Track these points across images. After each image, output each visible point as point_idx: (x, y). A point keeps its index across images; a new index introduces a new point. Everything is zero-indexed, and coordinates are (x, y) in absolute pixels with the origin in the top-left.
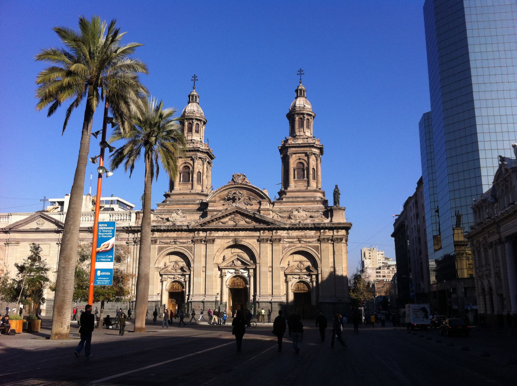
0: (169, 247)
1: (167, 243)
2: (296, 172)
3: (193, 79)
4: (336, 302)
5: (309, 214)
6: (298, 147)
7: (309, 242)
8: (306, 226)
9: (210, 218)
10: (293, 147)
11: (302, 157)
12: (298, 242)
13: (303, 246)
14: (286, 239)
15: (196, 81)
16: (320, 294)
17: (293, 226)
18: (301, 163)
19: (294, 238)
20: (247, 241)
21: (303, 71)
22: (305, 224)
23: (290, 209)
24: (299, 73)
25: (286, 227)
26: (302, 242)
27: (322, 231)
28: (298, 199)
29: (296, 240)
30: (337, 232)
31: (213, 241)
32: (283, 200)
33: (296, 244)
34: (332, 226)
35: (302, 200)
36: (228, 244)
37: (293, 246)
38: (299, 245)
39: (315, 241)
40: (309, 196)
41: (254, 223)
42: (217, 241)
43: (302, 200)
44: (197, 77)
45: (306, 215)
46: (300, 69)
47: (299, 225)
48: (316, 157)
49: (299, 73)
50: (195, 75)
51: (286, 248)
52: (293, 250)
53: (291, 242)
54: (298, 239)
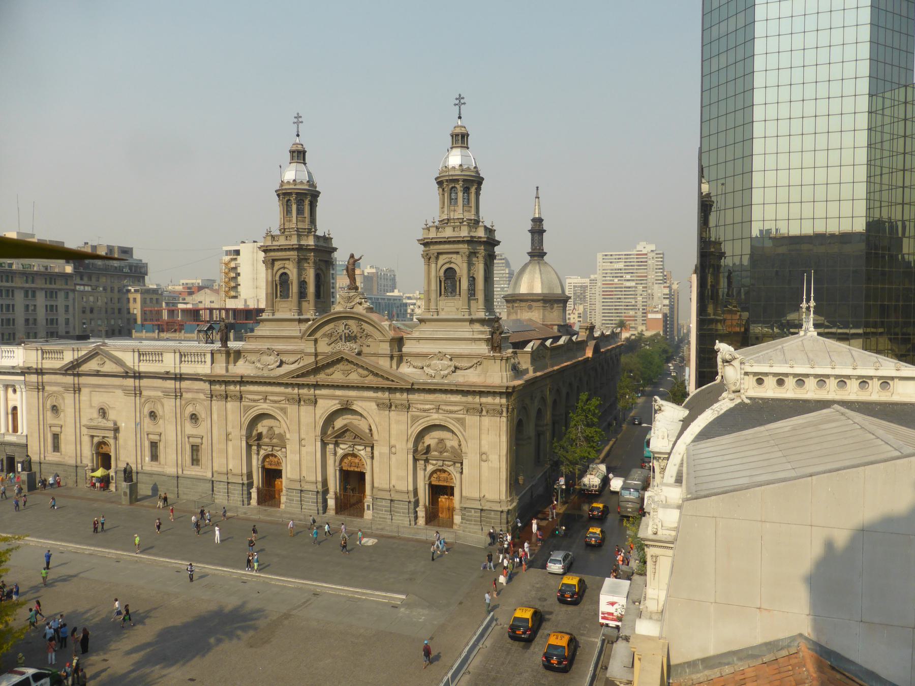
0: (257, 406)
1: (254, 401)
3: (296, 120)
7: (451, 412)
10: (436, 243)
11: (453, 260)
15: (300, 125)
20: (360, 403)
21: (463, 98)
24: (457, 102)
26: (440, 411)
38: (435, 416)
41: (371, 377)
42: (320, 402)
44: (301, 117)
46: (460, 95)
49: (457, 102)
50: (298, 114)
53: (425, 411)
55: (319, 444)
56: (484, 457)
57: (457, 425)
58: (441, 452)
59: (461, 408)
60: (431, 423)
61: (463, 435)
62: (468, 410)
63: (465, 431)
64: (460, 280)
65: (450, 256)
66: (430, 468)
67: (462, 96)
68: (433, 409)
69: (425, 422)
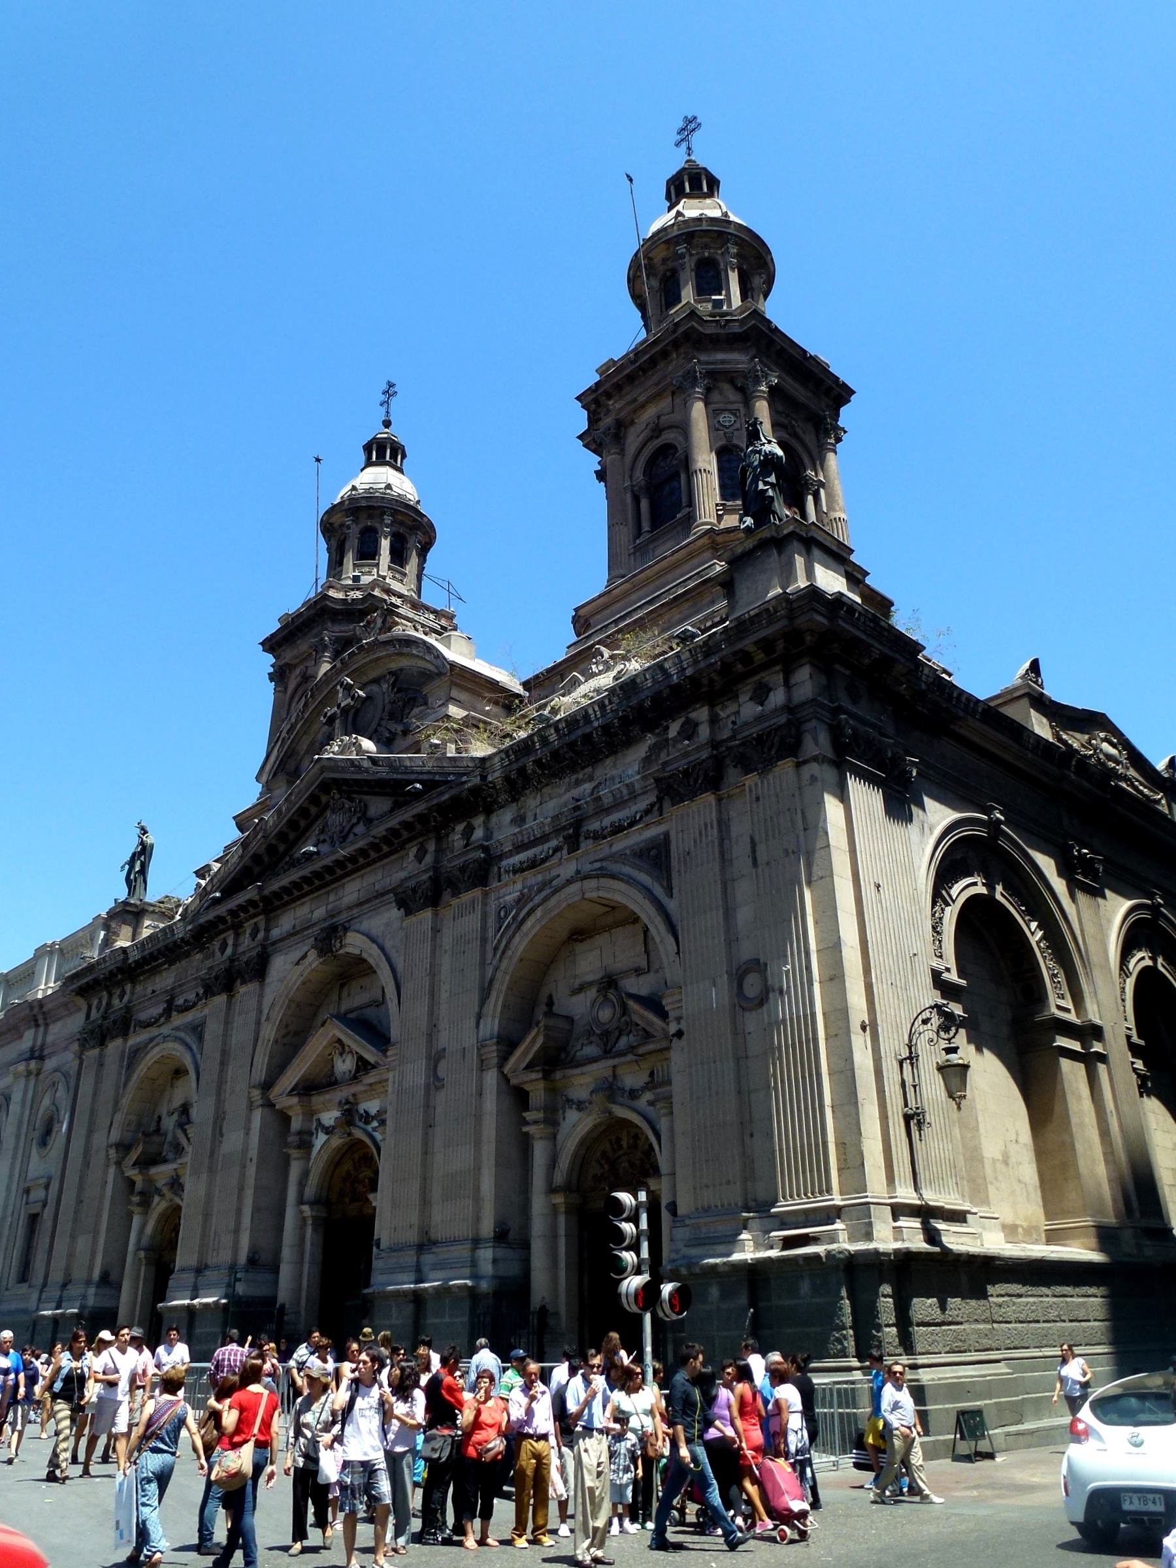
1: (147, 1025)
7: (618, 829)
8: (579, 732)
9: (241, 857)
13: (587, 868)
14: (511, 854)
17: (520, 764)
19: (544, 838)
27: (674, 729)
29: (554, 843)
31: (259, 969)
36: (300, 968)
37: (540, 891)
39: (647, 812)
47: (545, 741)
48: (742, 390)
51: (506, 916)
52: (539, 912)
53: (533, 864)
55: (257, 1116)
59: (652, 798)
65: (650, 412)
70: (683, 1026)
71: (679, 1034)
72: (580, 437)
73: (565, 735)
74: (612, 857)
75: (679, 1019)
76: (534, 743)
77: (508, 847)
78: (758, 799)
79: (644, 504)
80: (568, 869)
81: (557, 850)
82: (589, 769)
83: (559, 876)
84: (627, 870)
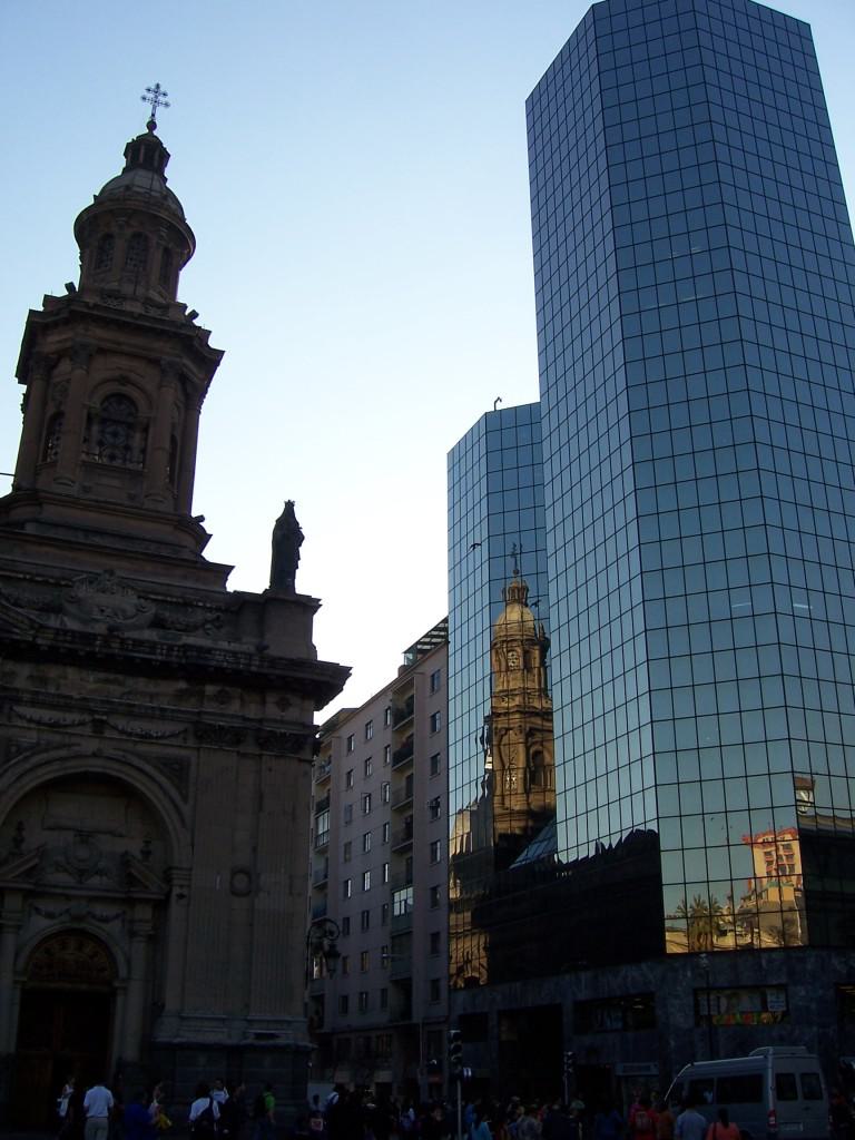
2: (95, 428)
4: (249, 1041)
5: (151, 610)
6: (121, 326)
7: (146, 737)
11: (133, 376)
12: (88, 730)
13: (109, 752)
16: (171, 1003)
18: (121, 397)
22: (138, 643)
23: (57, 573)
24: (151, 95)
25: (39, 641)
26: (107, 734)
27: (210, 689)
28: (97, 540)
30: (283, 704)
32: (23, 528)
33: (74, 740)
34: (265, 671)
35: (119, 545)
38: (91, 745)
39: (173, 735)
40: (148, 537)
43: (119, 545)
45: (140, 610)
46: (158, 86)
51: (19, 752)
52: (55, 766)
53: (54, 726)
54: (92, 712)
56: (241, 882)
57: (162, 779)
58: (82, 874)
59: (178, 727)
60: (74, 767)
61: (176, 807)
62: (206, 734)
63: (185, 799)
64: (146, 430)
65: (124, 363)
66: (40, 925)
67: (162, 89)
68: (82, 724)
69: (48, 762)
70: (185, 891)
71: (181, 896)
72: (32, 313)
73: (127, 650)
74: (139, 756)
75: (181, 886)
76: (96, 639)
77: (26, 697)
78: (270, 770)
79: (95, 428)
80: (91, 745)
81: (82, 724)
82: (121, 677)
83: (79, 745)
84: (148, 768)
